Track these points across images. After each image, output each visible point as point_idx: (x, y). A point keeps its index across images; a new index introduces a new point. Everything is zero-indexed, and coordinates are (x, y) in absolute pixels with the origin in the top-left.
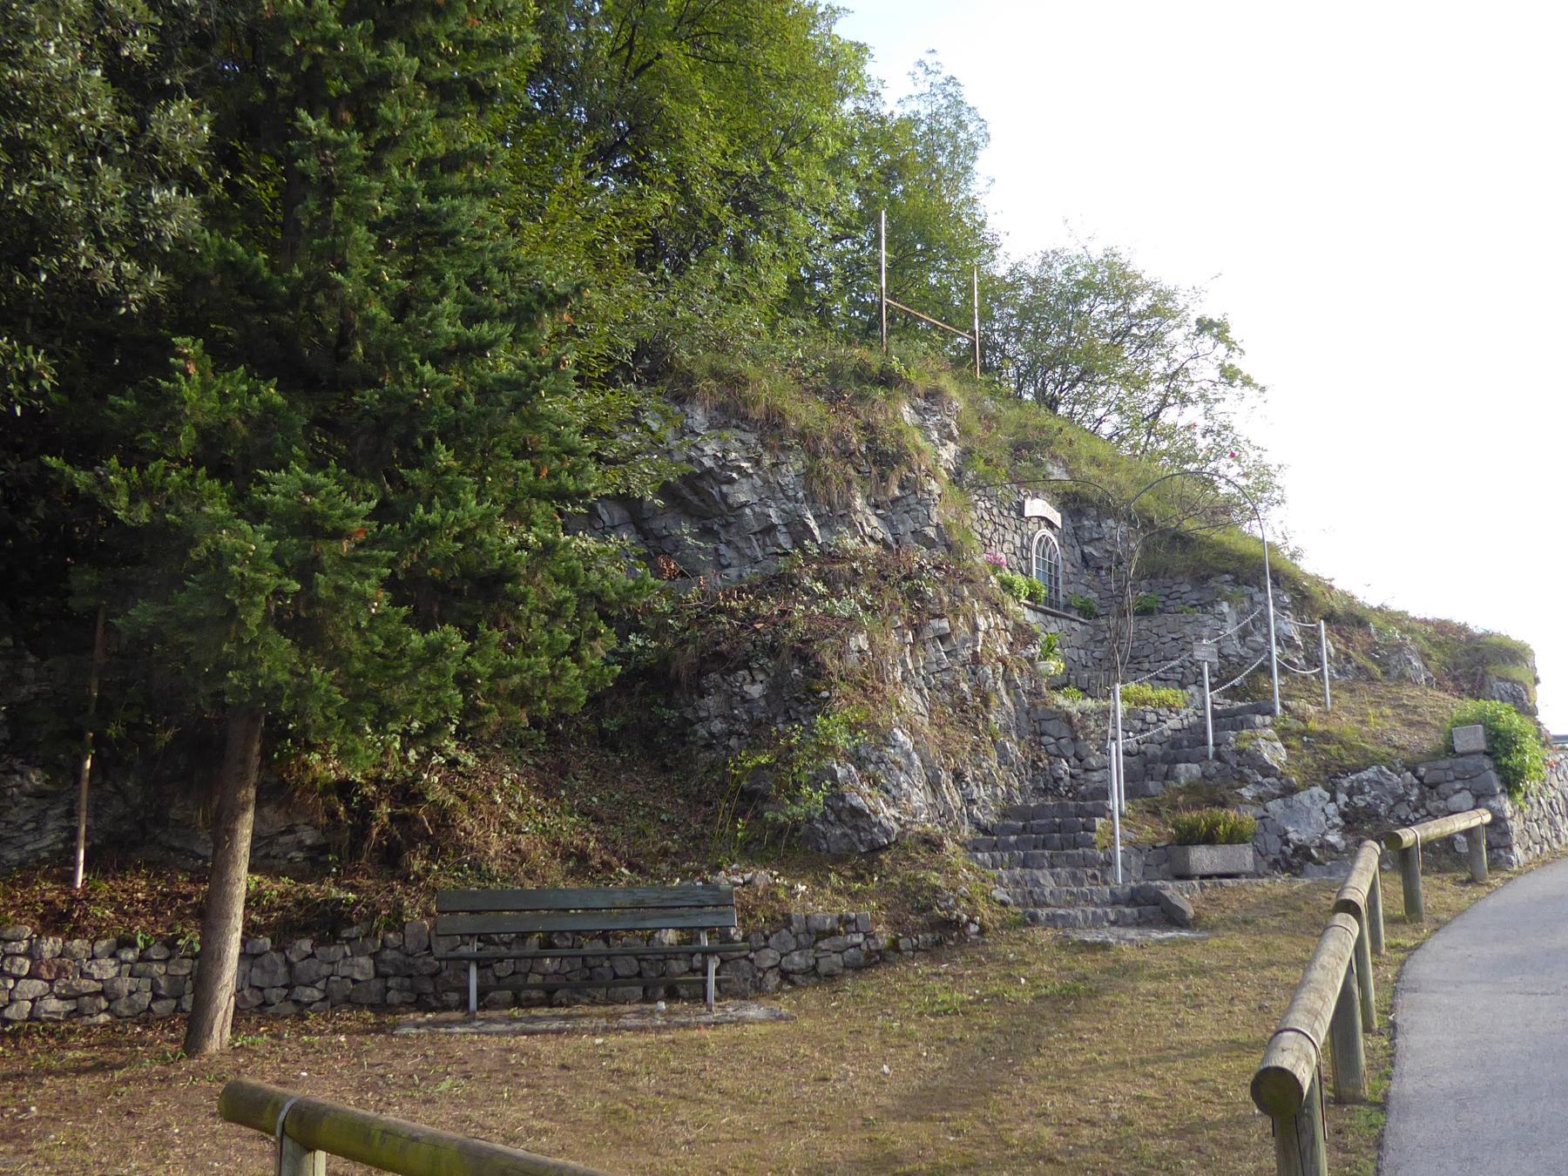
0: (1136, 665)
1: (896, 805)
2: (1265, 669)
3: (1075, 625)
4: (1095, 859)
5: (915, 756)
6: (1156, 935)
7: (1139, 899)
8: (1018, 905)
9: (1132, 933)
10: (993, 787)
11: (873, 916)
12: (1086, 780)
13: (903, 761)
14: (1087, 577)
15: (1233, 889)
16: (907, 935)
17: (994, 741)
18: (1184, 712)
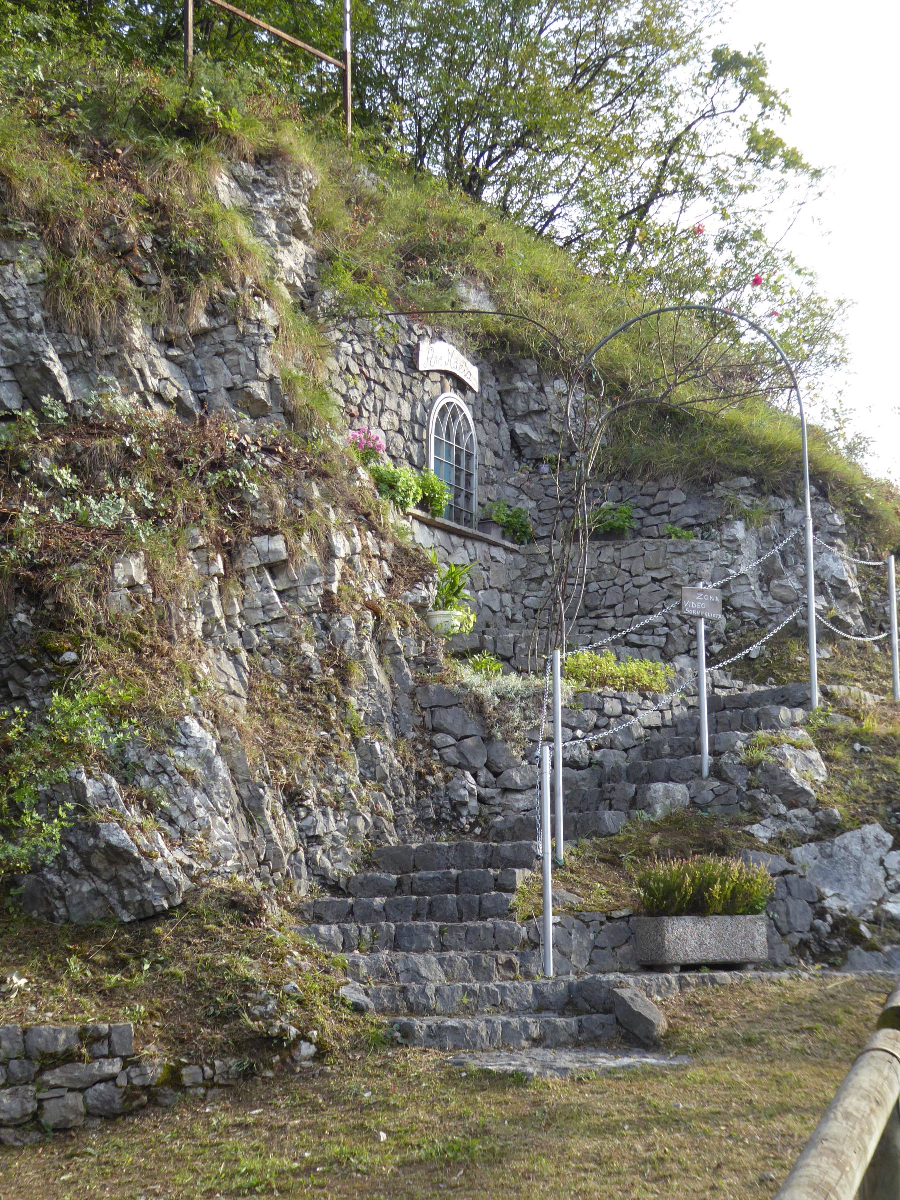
0: (592, 619)
1: (184, 844)
2: (798, 632)
3: (497, 553)
4: (513, 936)
5: (219, 763)
6: (605, 1061)
7: (580, 1002)
8: (382, 1011)
9: (566, 1059)
10: (352, 815)
11: (141, 1031)
12: (505, 807)
13: (200, 771)
14: (520, 474)
15: (732, 988)
16: (196, 1060)
17: (355, 741)
18: (665, 699)
